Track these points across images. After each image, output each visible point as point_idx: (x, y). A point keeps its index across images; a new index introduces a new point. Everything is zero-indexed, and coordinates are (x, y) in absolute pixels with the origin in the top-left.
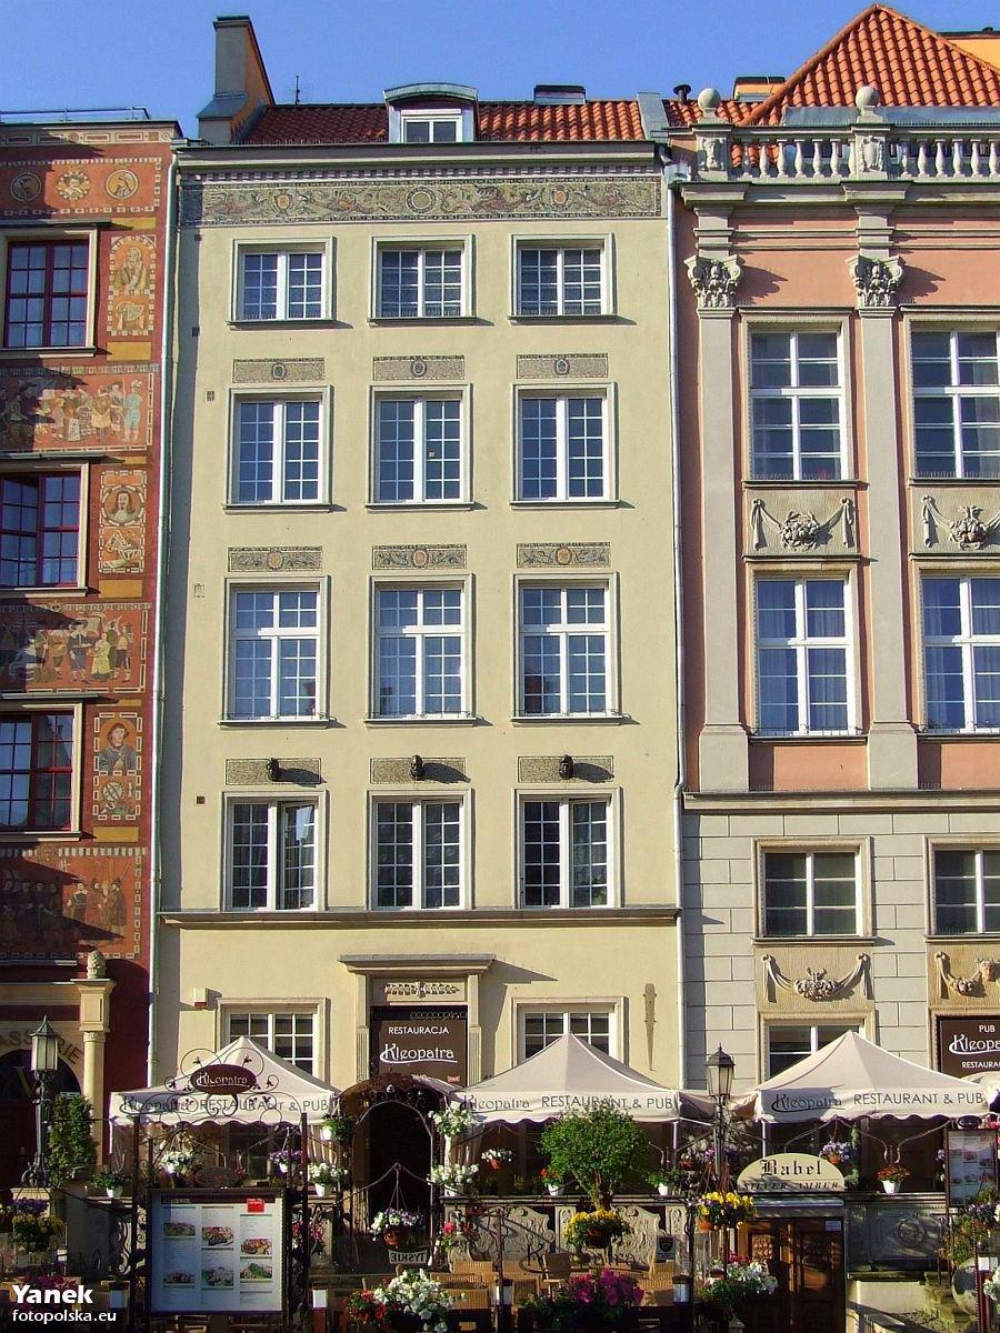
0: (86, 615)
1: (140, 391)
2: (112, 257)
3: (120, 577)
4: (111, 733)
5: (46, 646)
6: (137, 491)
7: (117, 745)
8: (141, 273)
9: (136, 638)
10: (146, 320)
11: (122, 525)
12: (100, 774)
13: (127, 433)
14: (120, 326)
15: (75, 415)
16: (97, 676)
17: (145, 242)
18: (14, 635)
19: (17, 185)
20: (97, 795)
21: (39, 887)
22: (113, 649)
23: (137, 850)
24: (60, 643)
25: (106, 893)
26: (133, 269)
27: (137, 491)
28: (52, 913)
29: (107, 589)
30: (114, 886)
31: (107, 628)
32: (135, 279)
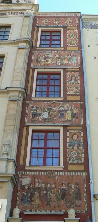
0: (63, 104)
1: (76, 56)
2: (67, 33)
3: (73, 95)
4: (72, 136)
5: (51, 112)
6: (77, 76)
7: (75, 140)
8: (74, 35)
9: (80, 110)
10: (76, 43)
11: (73, 83)
12: (69, 149)
13: (73, 64)
14: (70, 44)
15: (59, 60)
16: (68, 120)
17: (75, 30)
18: (41, 109)
19: (44, 21)
20: (69, 155)
21: (48, 185)
22: (72, 114)
23: (84, 173)
24: (56, 111)
25: (73, 188)
26: (73, 35)
27: (77, 76)
28: (53, 195)
29: (69, 98)
30: (76, 186)
31: (70, 108)
32: (73, 37)
